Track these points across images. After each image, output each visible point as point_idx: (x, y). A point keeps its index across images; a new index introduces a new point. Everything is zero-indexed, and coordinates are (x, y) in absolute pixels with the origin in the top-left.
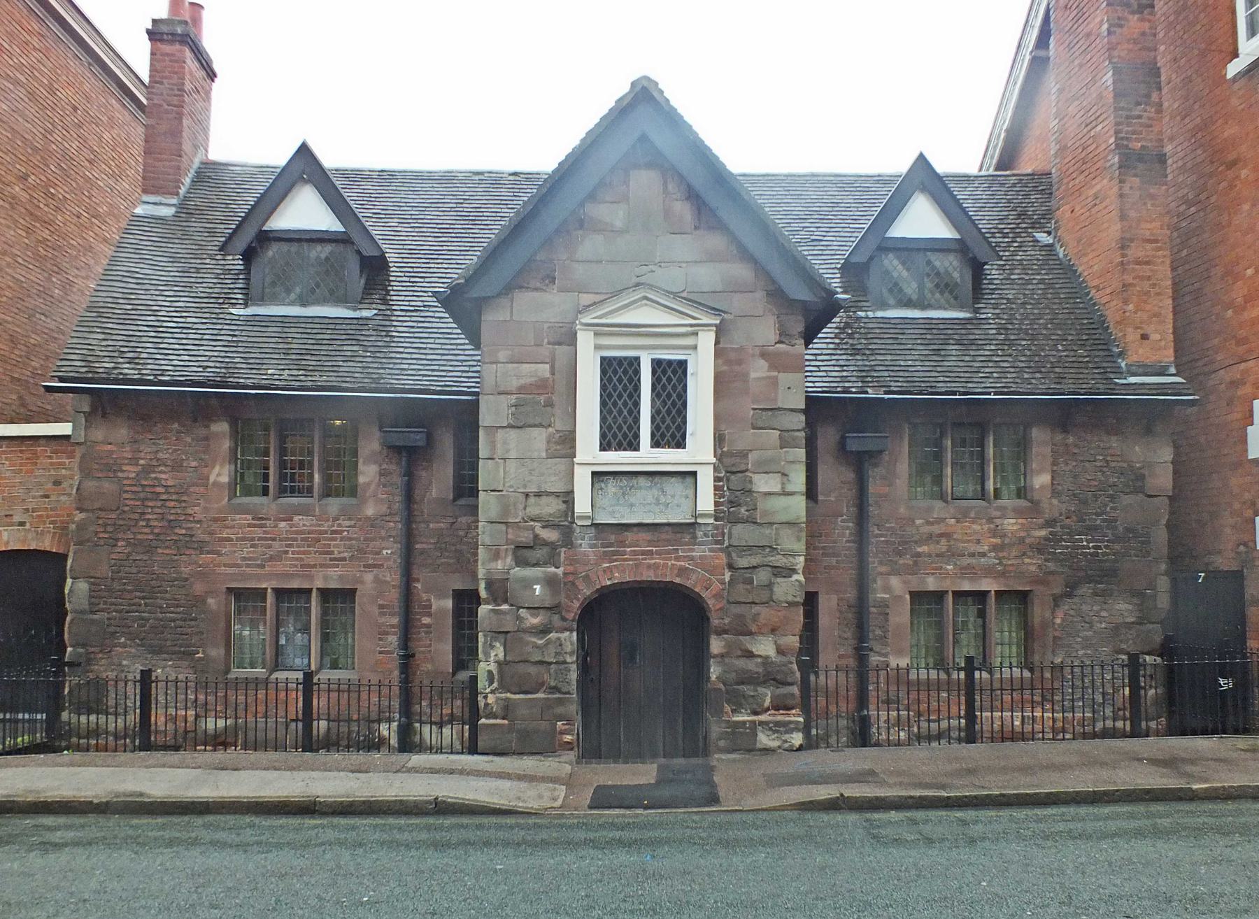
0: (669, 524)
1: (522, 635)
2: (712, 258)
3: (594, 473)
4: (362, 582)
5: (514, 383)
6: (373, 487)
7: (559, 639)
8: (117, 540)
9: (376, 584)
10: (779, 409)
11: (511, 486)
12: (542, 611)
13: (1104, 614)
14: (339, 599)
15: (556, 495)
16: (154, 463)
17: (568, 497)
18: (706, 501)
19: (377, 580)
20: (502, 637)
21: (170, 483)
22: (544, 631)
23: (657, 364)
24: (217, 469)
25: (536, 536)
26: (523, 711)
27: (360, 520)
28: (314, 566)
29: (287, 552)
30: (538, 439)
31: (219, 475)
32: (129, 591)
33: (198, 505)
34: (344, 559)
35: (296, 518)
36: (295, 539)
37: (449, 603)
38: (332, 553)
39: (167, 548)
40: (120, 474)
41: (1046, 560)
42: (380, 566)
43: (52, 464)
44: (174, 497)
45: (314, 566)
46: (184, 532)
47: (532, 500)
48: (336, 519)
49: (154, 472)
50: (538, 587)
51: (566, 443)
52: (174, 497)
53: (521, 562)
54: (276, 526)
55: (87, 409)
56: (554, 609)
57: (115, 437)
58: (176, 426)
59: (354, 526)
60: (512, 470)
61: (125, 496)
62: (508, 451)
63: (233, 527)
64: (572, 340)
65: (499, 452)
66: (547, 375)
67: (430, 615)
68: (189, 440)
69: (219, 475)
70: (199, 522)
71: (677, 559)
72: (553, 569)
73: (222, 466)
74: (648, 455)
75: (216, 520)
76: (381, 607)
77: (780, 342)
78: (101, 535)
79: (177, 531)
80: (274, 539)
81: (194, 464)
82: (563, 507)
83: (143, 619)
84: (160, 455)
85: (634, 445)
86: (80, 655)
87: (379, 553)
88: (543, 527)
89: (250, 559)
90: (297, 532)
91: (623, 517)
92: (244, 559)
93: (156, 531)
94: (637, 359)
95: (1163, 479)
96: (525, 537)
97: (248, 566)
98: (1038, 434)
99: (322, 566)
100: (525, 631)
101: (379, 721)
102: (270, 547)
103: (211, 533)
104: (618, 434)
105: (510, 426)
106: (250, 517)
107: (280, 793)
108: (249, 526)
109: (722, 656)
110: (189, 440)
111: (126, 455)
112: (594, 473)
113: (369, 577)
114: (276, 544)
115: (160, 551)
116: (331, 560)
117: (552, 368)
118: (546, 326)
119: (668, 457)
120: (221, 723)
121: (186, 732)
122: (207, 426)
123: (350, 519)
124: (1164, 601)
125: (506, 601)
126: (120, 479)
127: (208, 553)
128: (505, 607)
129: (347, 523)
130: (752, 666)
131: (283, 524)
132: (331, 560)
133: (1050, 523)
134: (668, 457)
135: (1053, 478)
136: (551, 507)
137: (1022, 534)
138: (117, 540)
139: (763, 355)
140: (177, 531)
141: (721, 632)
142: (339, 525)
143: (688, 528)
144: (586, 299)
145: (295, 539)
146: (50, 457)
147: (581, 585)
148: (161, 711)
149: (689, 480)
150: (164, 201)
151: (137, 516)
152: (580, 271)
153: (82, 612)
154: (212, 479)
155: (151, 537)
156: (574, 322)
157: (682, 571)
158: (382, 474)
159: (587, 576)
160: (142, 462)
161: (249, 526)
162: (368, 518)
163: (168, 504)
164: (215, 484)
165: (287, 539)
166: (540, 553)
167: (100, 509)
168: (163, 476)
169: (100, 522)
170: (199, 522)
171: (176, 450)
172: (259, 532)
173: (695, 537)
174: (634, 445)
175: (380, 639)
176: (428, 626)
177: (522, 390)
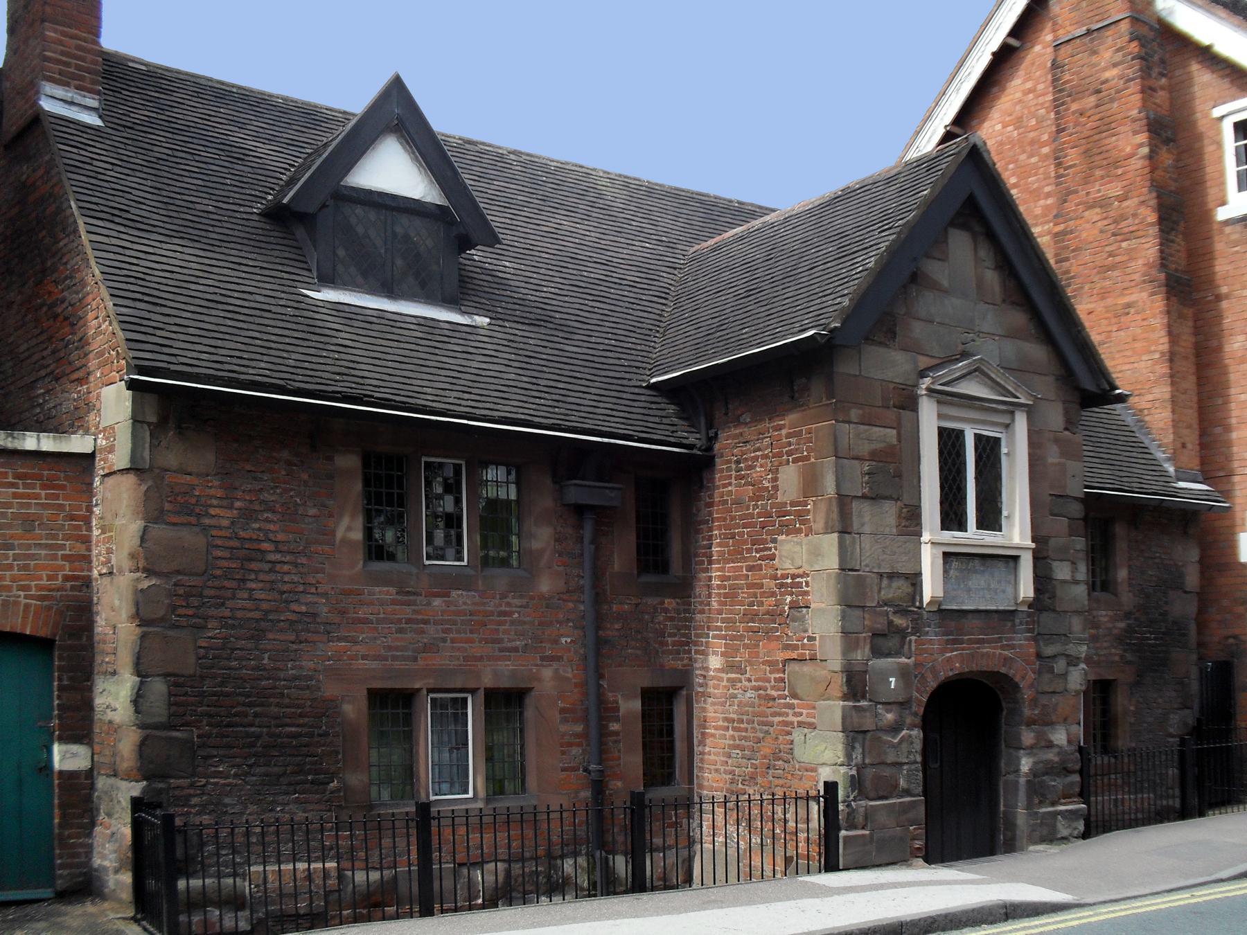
0: (996, 611)
1: (880, 734)
2: (1012, 334)
3: (945, 554)
4: (539, 680)
5: (865, 448)
6: (546, 556)
7: (910, 736)
8: (206, 618)
9: (553, 680)
10: (1067, 496)
11: (867, 566)
12: (894, 707)
13: (1160, 700)
14: (506, 703)
15: (906, 577)
16: (257, 507)
17: (915, 579)
18: (1026, 588)
19: (557, 677)
20: (860, 737)
21: (281, 537)
22: (895, 728)
23: (978, 438)
24: (345, 521)
25: (890, 623)
26: (882, 818)
27: (532, 598)
28: (481, 658)
29: (444, 640)
30: (890, 511)
31: (349, 529)
32: (227, 695)
33: (322, 571)
34: (516, 650)
35: (454, 593)
36: (455, 623)
37: (637, 705)
38: (500, 641)
39: (281, 630)
40: (207, 521)
41: (1125, 651)
42: (559, 659)
43: (15, 496)
44: (288, 558)
45: (481, 658)
46: (304, 609)
47: (885, 582)
48: (503, 596)
49: (257, 520)
50: (893, 680)
51: (911, 520)
52: (288, 558)
53: (877, 652)
54: (429, 604)
55: (153, 419)
56: (904, 705)
57: (193, 462)
58: (285, 454)
59: (526, 606)
60: (868, 547)
61: (219, 553)
62: (863, 525)
63: (372, 603)
64: (911, 404)
65: (856, 526)
66: (894, 441)
67: (617, 720)
68: (305, 476)
69: (349, 529)
70: (325, 595)
71: (1003, 648)
72: (903, 660)
73: (353, 517)
74: (973, 536)
75: (348, 593)
76: (563, 711)
77: (1066, 429)
78: (181, 611)
79: (294, 607)
80: (426, 622)
81: (312, 512)
82: (910, 590)
83: (248, 735)
84: (265, 496)
85: (962, 526)
86: (160, 791)
87: (556, 642)
88: (895, 613)
89: (397, 649)
90: (459, 613)
91: (963, 603)
92: (390, 648)
93: (265, 606)
94: (960, 433)
95: (1192, 579)
96: (881, 624)
97: (394, 658)
98: (1120, 530)
99: (490, 658)
100: (881, 730)
101: (562, 857)
102: (423, 632)
103: (343, 612)
105: (864, 497)
106: (392, 590)
107: (838, 924)
108: (394, 602)
109: (1031, 747)
110: (305, 476)
111: (212, 492)
112: (945, 554)
113: (547, 673)
114: (431, 629)
115: (270, 636)
116: (501, 650)
117: (899, 434)
118: (892, 386)
119: (989, 538)
120: (375, 876)
121: (327, 894)
122: (331, 459)
123: (521, 597)
124: (1195, 687)
125: (864, 697)
126: (205, 529)
127: (339, 639)
128: (863, 703)
129: (517, 602)
130: (1051, 756)
131: (437, 602)
132: (501, 650)
133: (1128, 615)
134: (989, 538)
135: (1130, 573)
136: (898, 589)
137: (1110, 625)
138: (206, 618)
139: (1057, 441)
140: (294, 607)
141: (1030, 723)
142: (508, 604)
143: (1008, 615)
144: (924, 362)
145: (455, 623)
146: (13, 485)
147: (929, 677)
148: (446, 856)
149: (1012, 564)
150: (78, 99)
151: (234, 584)
152: (918, 330)
153: (156, 727)
154: (340, 534)
155: (256, 615)
156: (916, 386)
157: (1006, 660)
158: (559, 539)
159: (933, 666)
160: (238, 504)
161: (394, 602)
162: (542, 597)
163: (278, 567)
164: (344, 541)
165: (441, 622)
166: (893, 642)
167: (178, 572)
168: (272, 527)
169: (181, 592)
170: (325, 595)
171: (286, 491)
172: (407, 612)
173: (1014, 625)
174: (962, 526)
175: (563, 753)
176: (617, 733)
177: (874, 456)
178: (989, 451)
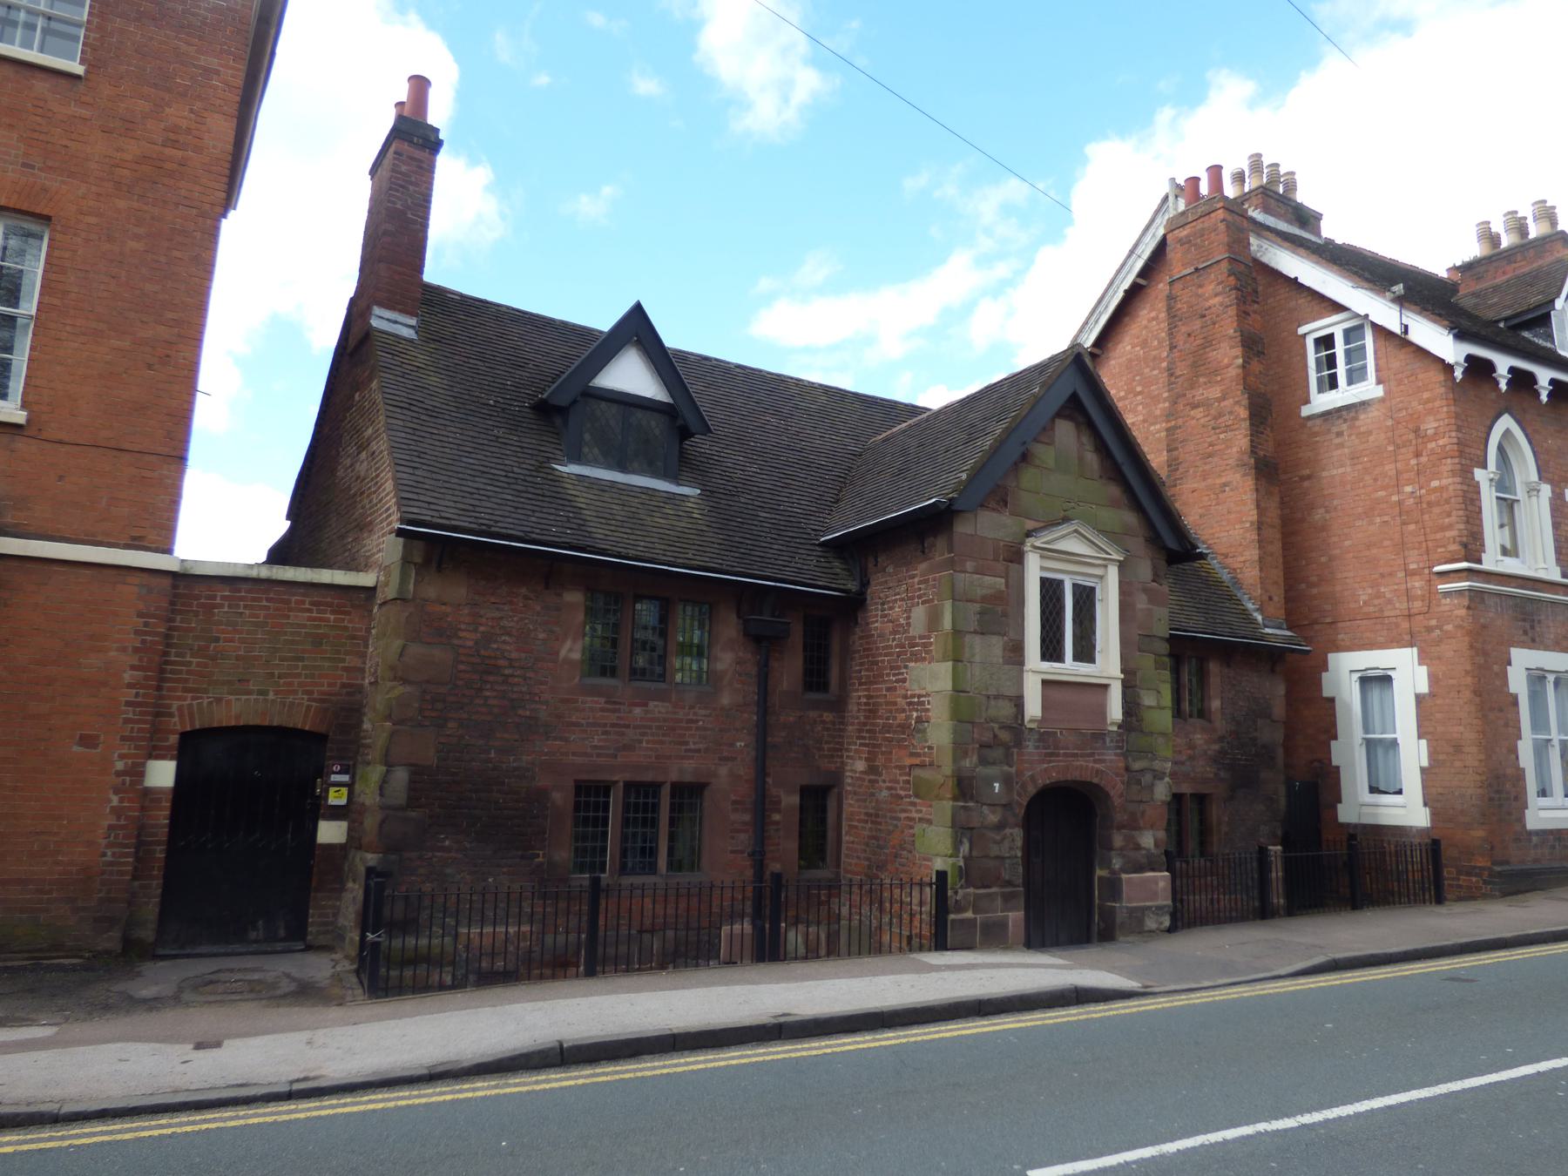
14: (689, 794)
15: (1010, 698)
17: (1018, 702)
21: (514, 655)
22: (1000, 826)
24: (568, 644)
25: (995, 736)
30: (996, 645)
34: (698, 751)
35: (652, 704)
37: (795, 799)
40: (456, 642)
42: (733, 759)
45: (669, 757)
48: (691, 707)
50: (997, 785)
51: (1016, 652)
53: (983, 761)
55: (418, 560)
56: (1007, 806)
57: (451, 594)
58: (523, 590)
61: (462, 667)
64: (1017, 557)
66: (1003, 588)
67: (779, 811)
69: (570, 650)
71: (1095, 761)
72: (1006, 768)
76: (734, 802)
79: (520, 712)
84: (505, 623)
87: (732, 745)
90: (653, 720)
92: (595, 747)
94: (1061, 582)
95: (1279, 710)
96: (987, 737)
97: (598, 755)
98: (1214, 667)
104: (1051, 650)
105: (975, 632)
106: (603, 700)
108: (602, 710)
109: (1121, 849)
113: (723, 771)
122: (560, 595)
124: (1283, 802)
125: (972, 798)
127: (555, 739)
128: (971, 804)
129: (703, 712)
131: (638, 711)
133: (1221, 739)
136: (1006, 710)
139: (1145, 590)
140: (520, 712)
141: (1121, 827)
144: (1030, 525)
154: (563, 653)
156: (1023, 543)
160: (482, 629)
161: (602, 710)
166: (998, 753)
171: (522, 619)
176: (777, 823)
177: (984, 599)
178: (1086, 598)
